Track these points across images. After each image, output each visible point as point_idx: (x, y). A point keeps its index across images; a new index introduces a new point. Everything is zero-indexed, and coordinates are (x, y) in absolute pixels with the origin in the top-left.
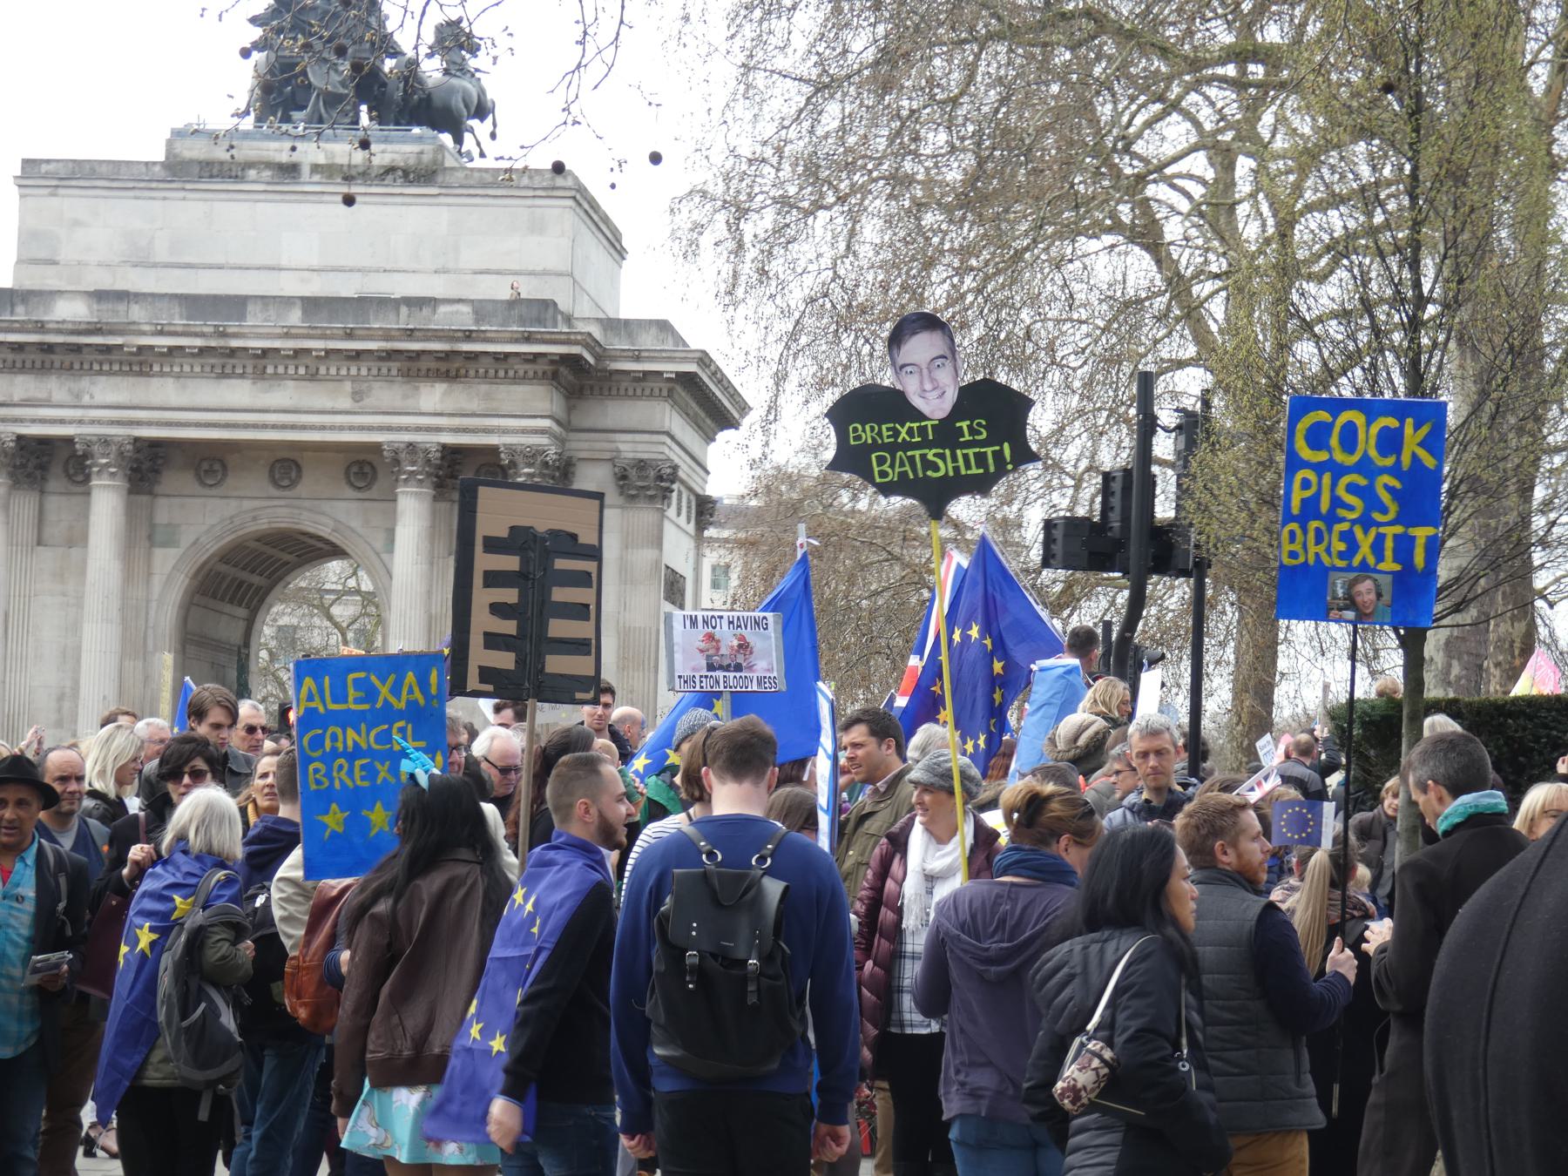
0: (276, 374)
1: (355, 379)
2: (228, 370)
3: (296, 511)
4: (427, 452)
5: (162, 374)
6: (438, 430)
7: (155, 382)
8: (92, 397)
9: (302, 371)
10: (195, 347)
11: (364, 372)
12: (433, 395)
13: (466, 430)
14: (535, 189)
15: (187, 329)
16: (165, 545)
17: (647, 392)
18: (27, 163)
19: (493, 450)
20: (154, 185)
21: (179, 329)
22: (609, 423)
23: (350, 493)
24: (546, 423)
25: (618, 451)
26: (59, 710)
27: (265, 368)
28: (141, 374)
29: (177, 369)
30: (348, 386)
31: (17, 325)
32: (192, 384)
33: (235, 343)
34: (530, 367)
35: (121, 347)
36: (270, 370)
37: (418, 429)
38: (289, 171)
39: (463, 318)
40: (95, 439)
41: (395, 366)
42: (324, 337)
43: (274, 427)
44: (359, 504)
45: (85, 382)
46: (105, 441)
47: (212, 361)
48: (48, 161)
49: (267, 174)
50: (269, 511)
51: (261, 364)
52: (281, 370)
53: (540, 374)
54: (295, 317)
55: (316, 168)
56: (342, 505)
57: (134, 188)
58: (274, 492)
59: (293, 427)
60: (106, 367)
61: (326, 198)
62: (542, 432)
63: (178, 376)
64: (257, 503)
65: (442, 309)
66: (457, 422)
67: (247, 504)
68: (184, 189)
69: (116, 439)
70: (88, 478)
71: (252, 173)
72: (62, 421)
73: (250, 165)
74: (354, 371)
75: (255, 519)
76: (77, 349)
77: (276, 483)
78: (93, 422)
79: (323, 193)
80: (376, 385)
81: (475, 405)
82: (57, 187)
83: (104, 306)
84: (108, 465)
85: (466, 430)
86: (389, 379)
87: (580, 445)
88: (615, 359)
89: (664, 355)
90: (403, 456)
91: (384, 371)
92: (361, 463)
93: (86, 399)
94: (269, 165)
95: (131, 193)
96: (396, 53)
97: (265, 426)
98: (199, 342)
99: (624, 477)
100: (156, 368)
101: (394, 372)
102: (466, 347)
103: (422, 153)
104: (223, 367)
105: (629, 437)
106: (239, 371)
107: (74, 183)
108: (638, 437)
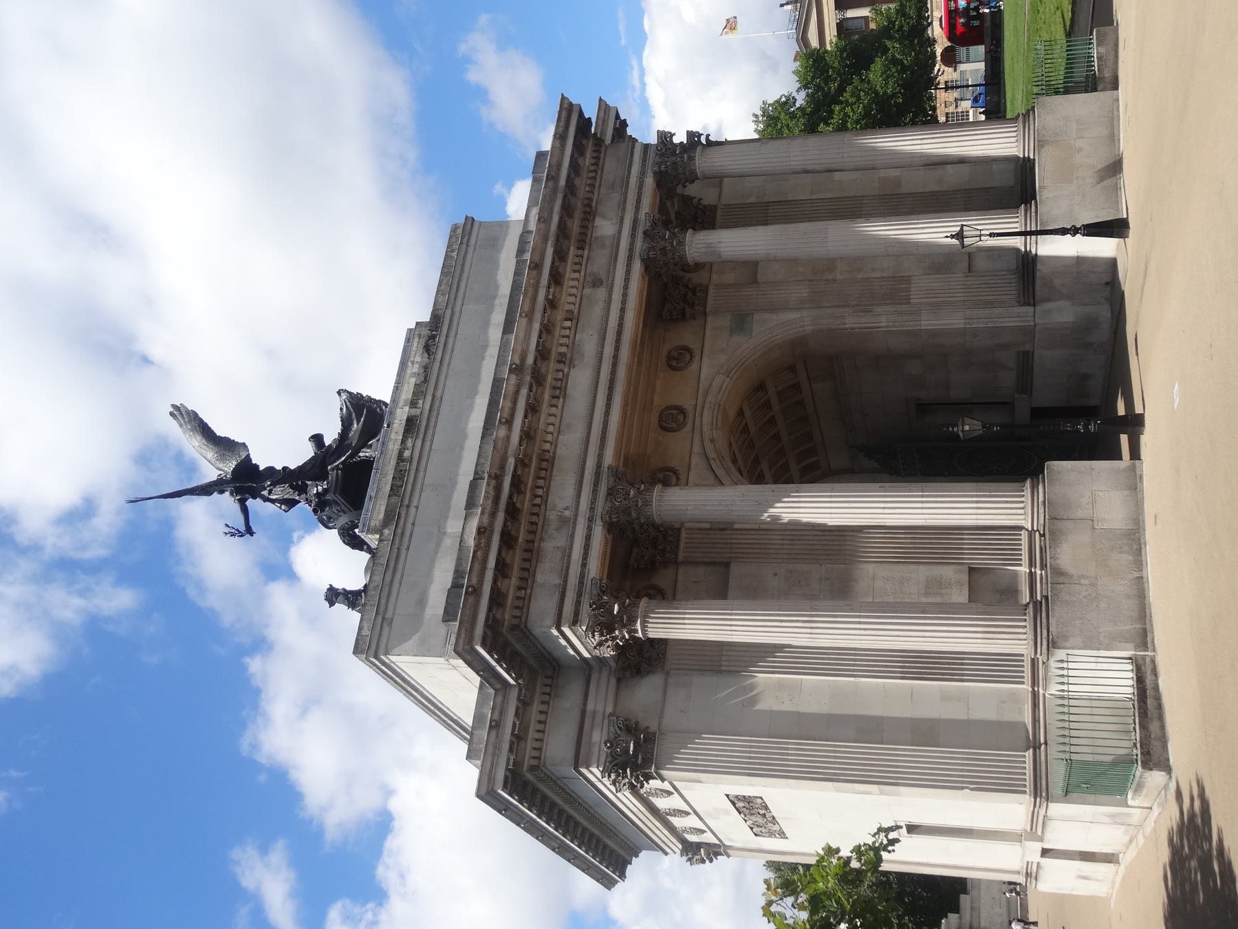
3: (707, 406)
5: (555, 444)
6: (635, 222)
7: (561, 451)
8: (567, 508)
9: (568, 324)
12: (604, 227)
15: (509, 398)
20: (399, 531)
21: (509, 404)
23: (694, 366)
28: (552, 461)
29: (551, 428)
31: (479, 553)
33: (530, 360)
38: (411, 423)
40: (609, 504)
43: (617, 349)
44: (705, 359)
45: (552, 516)
46: (611, 493)
47: (547, 396)
48: (360, 628)
49: (409, 443)
50: (705, 428)
58: (689, 426)
59: (619, 333)
61: (438, 394)
68: (408, 506)
69: (611, 484)
71: (407, 454)
72: (588, 538)
78: (592, 509)
79: (434, 396)
81: (616, 197)
82: (383, 618)
94: (403, 442)
95: (403, 552)
97: (616, 357)
100: (547, 446)
102: (562, 182)
107: (383, 601)
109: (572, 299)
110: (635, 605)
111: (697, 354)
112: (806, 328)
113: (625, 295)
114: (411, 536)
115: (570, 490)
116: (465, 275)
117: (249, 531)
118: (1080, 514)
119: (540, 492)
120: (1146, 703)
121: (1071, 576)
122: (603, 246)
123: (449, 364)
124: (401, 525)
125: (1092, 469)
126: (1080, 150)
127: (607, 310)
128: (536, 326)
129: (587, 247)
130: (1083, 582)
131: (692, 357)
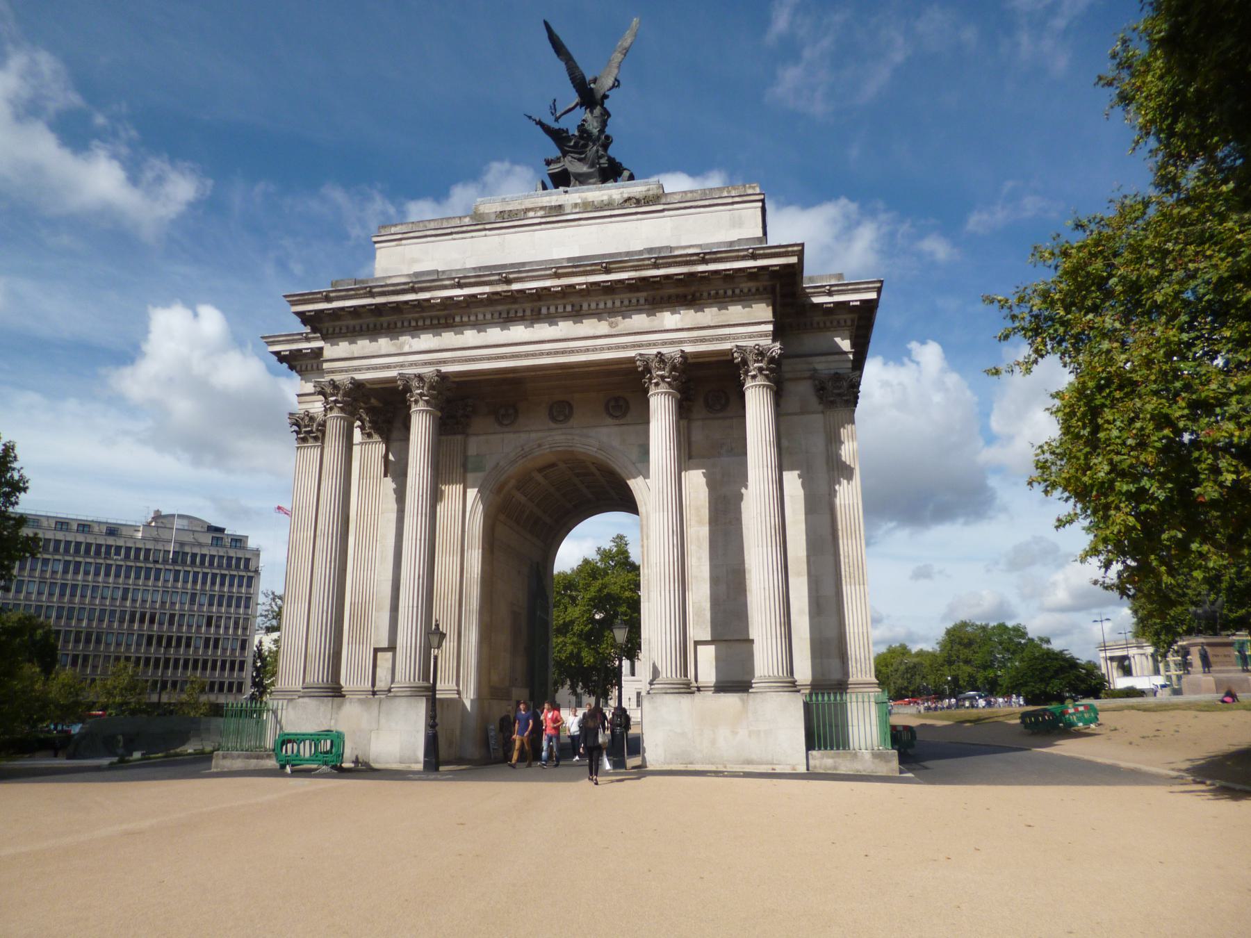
0: (549, 314)
2: (512, 314)
3: (569, 437)
6: (681, 342)
8: (410, 346)
9: (569, 308)
10: (484, 294)
11: (618, 303)
13: (702, 340)
14: (733, 197)
16: (476, 470)
17: (835, 323)
20: (464, 229)
23: (609, 421)
25: (815, 370)
27: (540, 310)
29: (473, 318)
33: (516, 286)
34: (752, 285)
36: (544, 311)
37: (664, 343)
38: (559, 209)
41: (642, 295)
46: (420, 377)
47: (500, 308)
49: (541, 213)
50: (549, 439)
52: (552, 309)
53: (761, 289)
56: (605, 430)
57: (451, 234)
58: (553, 425)
60: (420, 323)
64: (540, 434)
67: (533, 435)
68: (485, 230)
70: (410, 407)
71: (531, 214)
72: (388, 367)
73: (527, 210)
74: (609, 304)
75: (540, 446)
76: (398, 308)
77: (553, 419)
82: (401, 239)
84: (421, 395)
85: (702, 340)
89: (850, 287)
91: (634, 301)
92: (617, 399)
93: (406, 349)
94: (542, 208)
95: (450, 237)
98: (487, 289)
99: (823, 389)
100: (458, 319)
101: (642, 301)
103: (649, 190)
104: (508, 313)
105: (823, 359)
106: (520, 314)
107: (412, 235)
109: (593, 306)
111: (622, 421)
112: (644, 508)
113: (602, 349)
114: (463, 238)
116: (702, 210)
118: (383, 721)
119: (420, 323)
120: (254, 758)
121: (337, 713)
123: (611, 222)
124: (470, 228)
125: (418, 732)
126: (734, 733)
129: (650, 307)
130: (333, 721)
131: (616, 417)
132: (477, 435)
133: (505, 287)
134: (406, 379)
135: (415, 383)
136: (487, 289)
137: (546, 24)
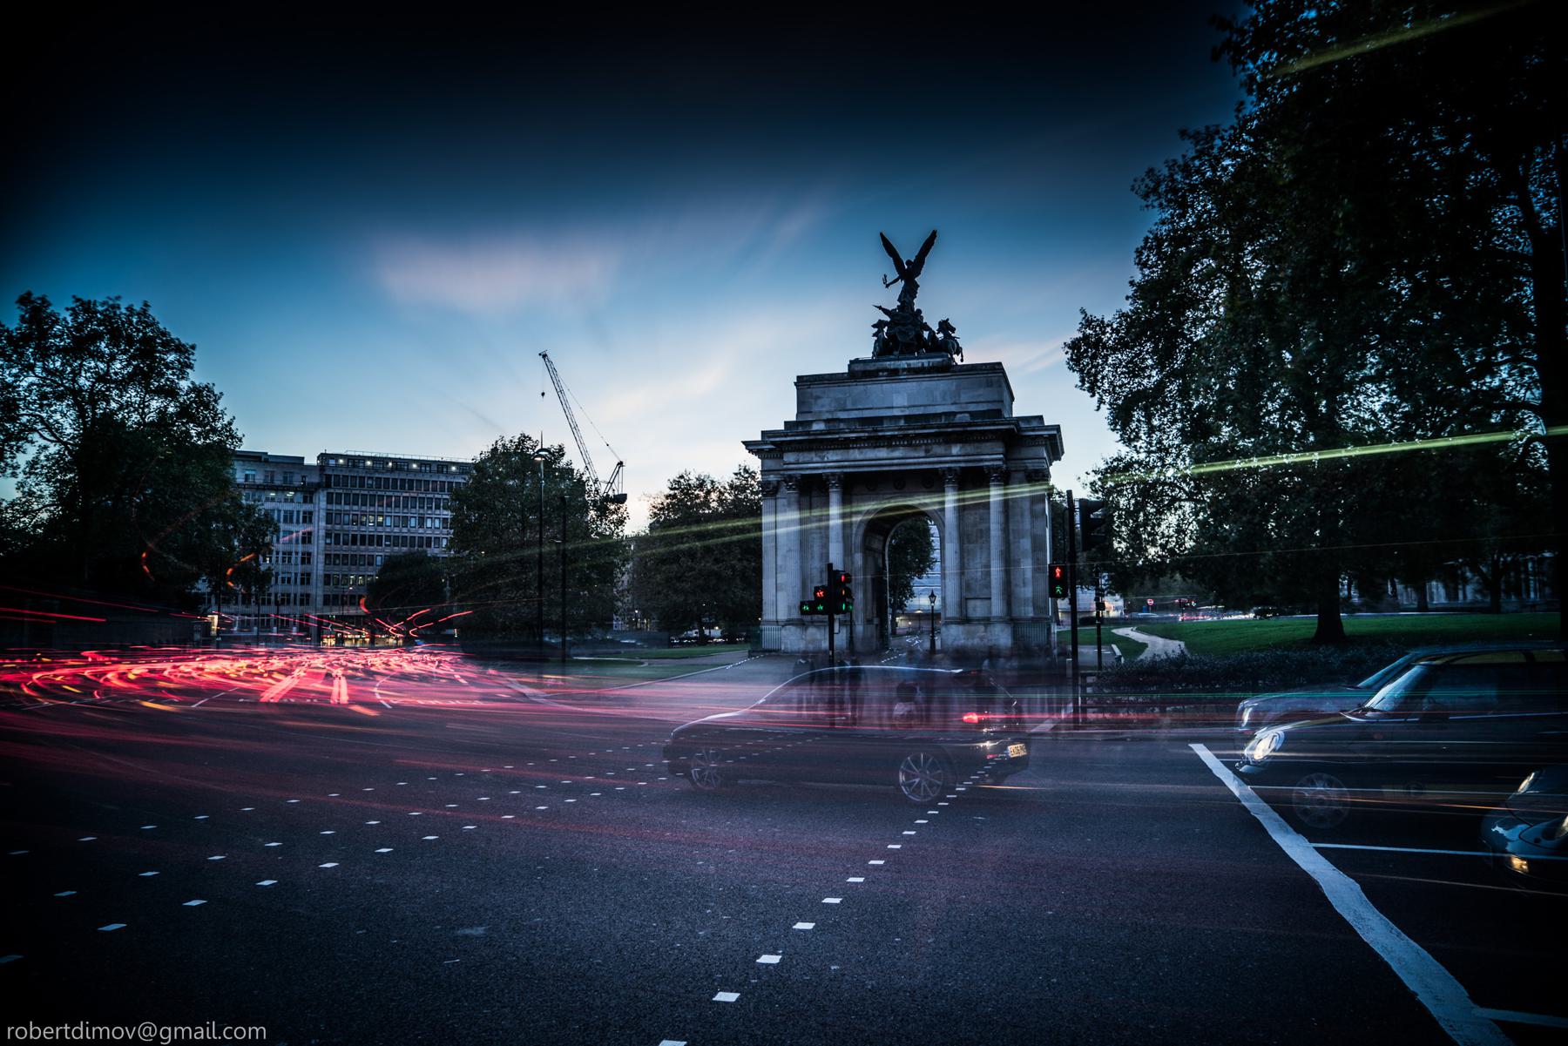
1: (926, 445)
4: (955, 470)
5: (853, 448)
6: (959, 462)
7: (851, 451)
9: (906, 443)
11: (929, 441)
12: (955, 450)
18: (798, 377)
19: (982, 467)
22: (1023, 456)
24: (1001, 456)
26: (821, 576)
30: (924, 447)
32: (864, 451)
33: (880, 434)
35: (837, 439)
36: (894, 443)
39: (967, 418)
42: (914, 429)
46: (833, 474)
49: (885, 373)
51: (889, 442)
54: (902, 423)
55: (904, 370)
62: (999, 460)
63: (859, 448)
65: (958, 416)
66: (966, 458)
70: (828, 489)
71: (881, 374)
73: (879, 371)
80: (934, 446)
83: (831, 424)
86: (939, 444)
87: (1012, 465)
88: (1025, 431)
90: (946, 472)
93: (826, 459)
96: (928, 329)
105: (1030, 461)
108: (1033, 461)
110: (794, 489)
115: (835, 458)
117: (887, 286)
122: (946, 450)
127: (915, 458)
128: (896, 433)
131: (927, 488)
132: (856, 495)
133: (875, 434)
134: (827, 475)
135: (831, 478)
136: (867, 434)
137: (881, 234)
